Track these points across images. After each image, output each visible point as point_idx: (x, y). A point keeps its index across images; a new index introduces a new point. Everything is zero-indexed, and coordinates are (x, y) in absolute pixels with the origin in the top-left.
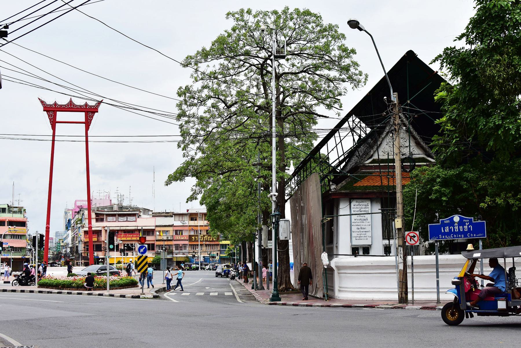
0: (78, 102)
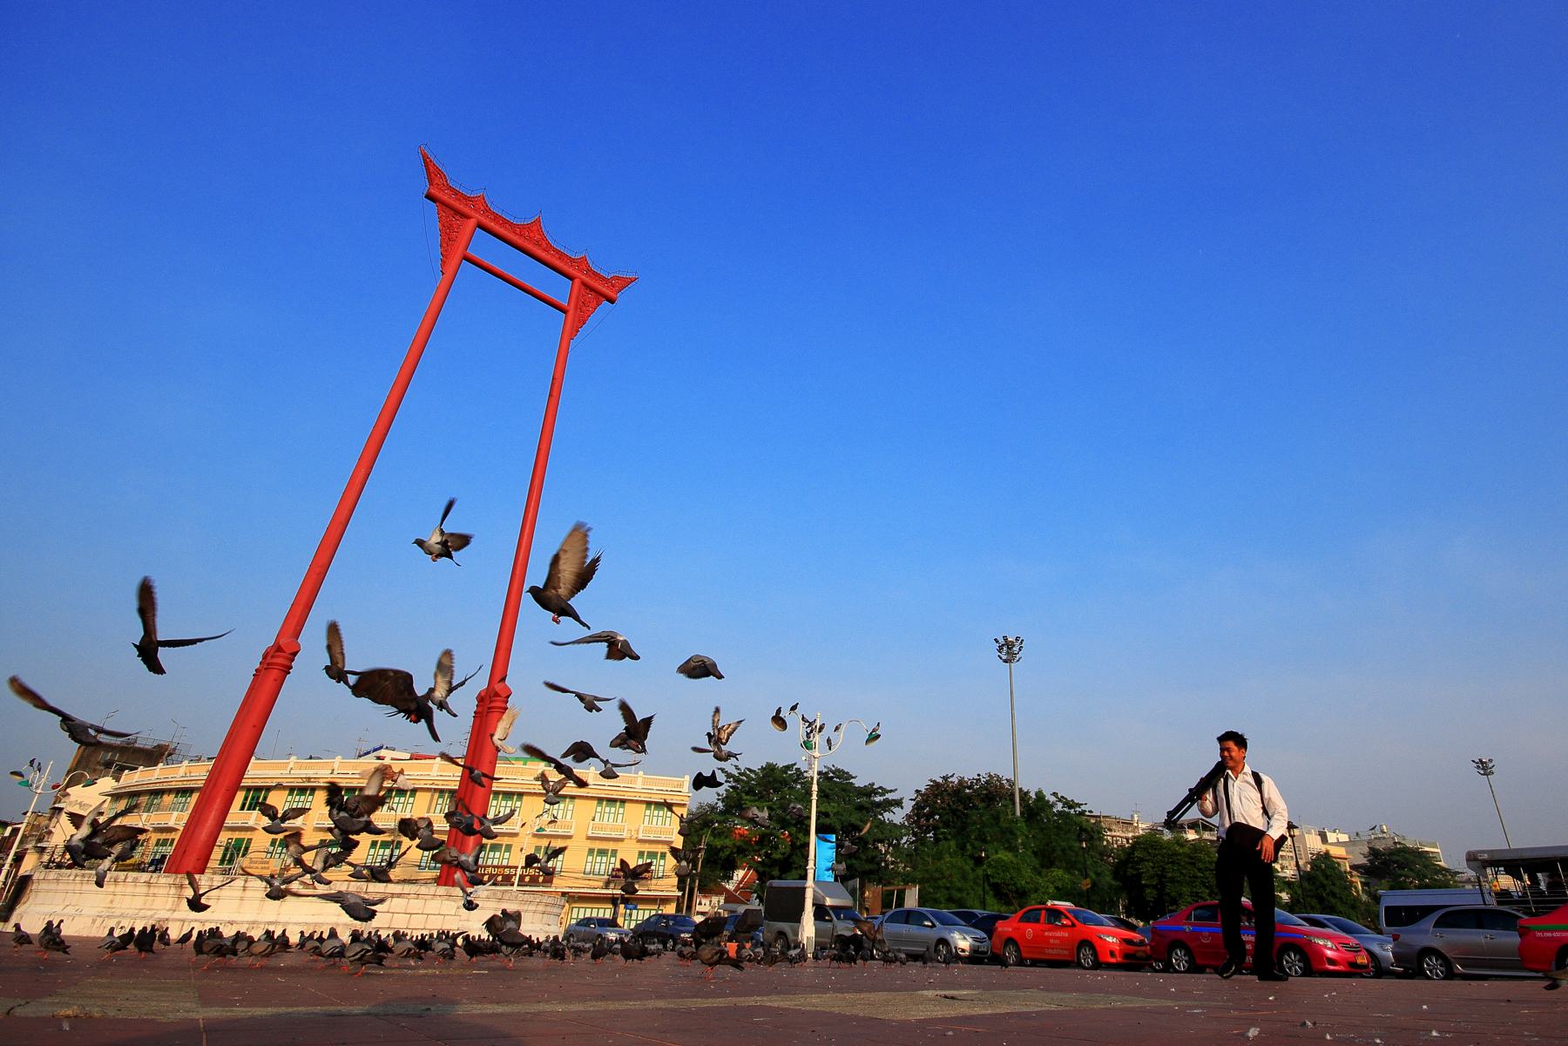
0: (565, 238)
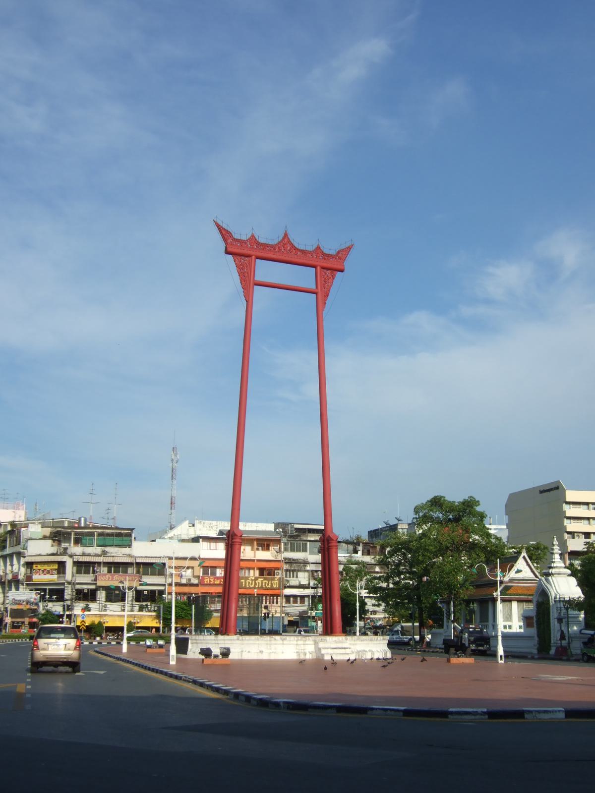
0: (303, 241)
